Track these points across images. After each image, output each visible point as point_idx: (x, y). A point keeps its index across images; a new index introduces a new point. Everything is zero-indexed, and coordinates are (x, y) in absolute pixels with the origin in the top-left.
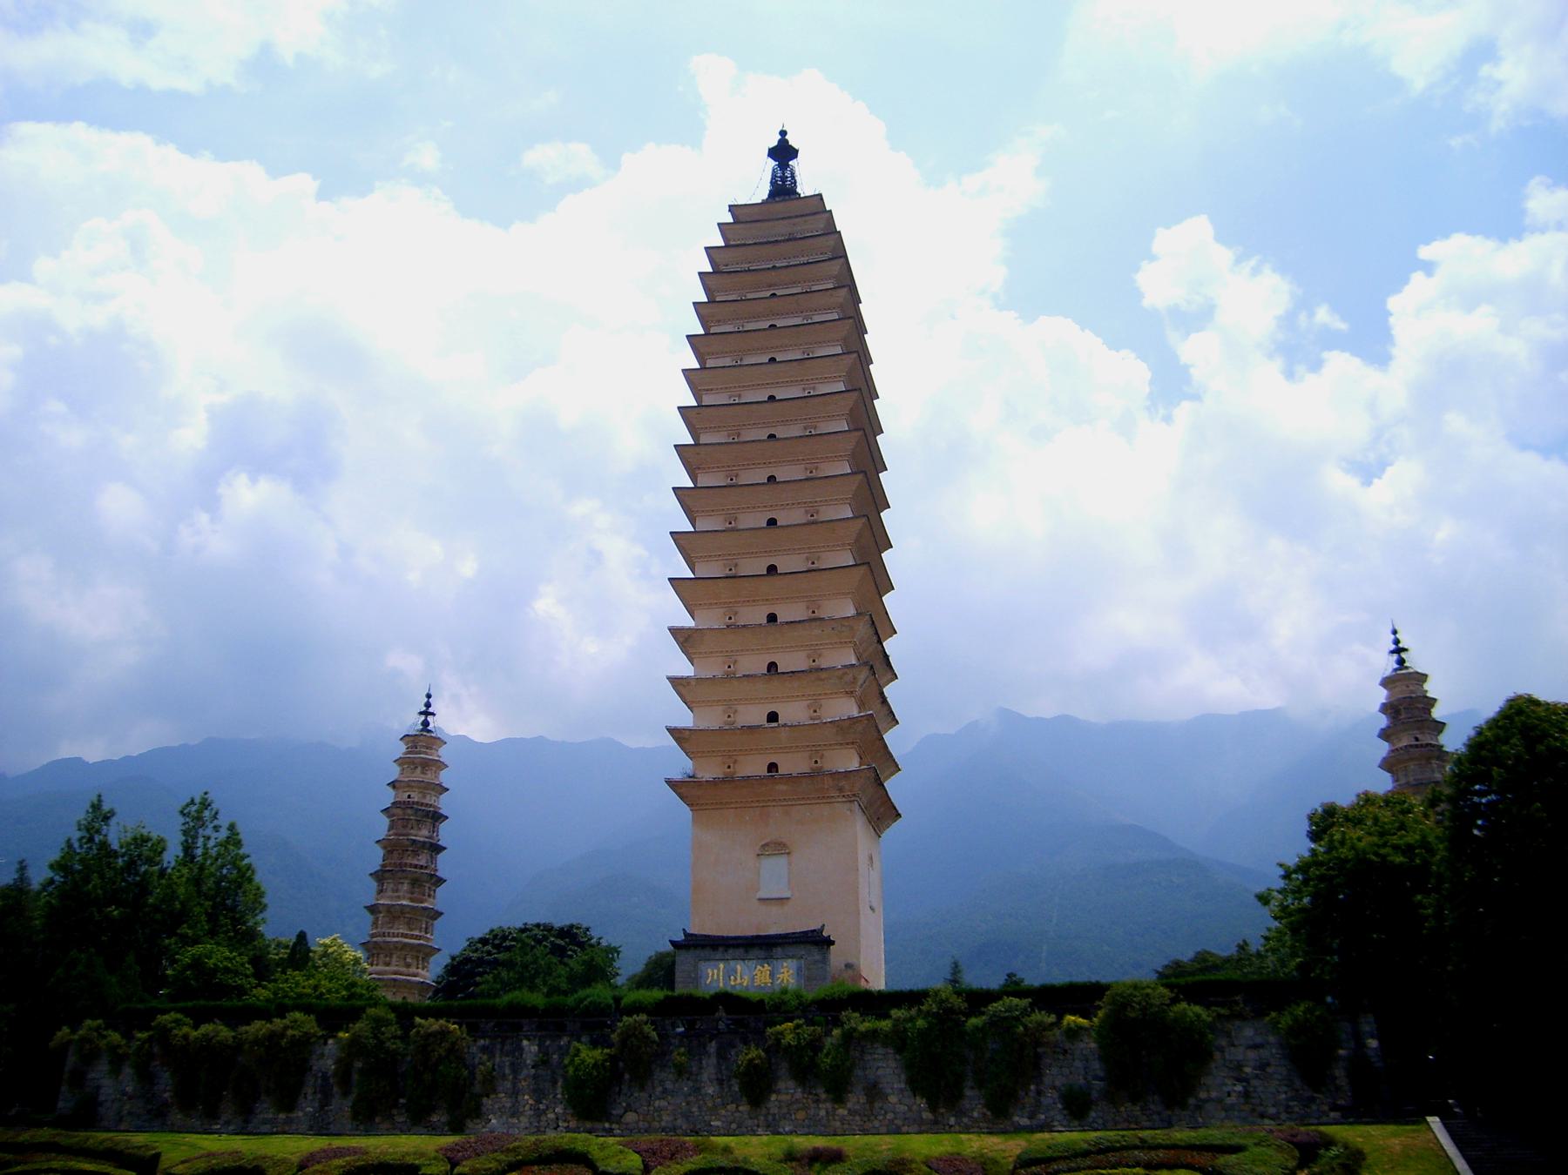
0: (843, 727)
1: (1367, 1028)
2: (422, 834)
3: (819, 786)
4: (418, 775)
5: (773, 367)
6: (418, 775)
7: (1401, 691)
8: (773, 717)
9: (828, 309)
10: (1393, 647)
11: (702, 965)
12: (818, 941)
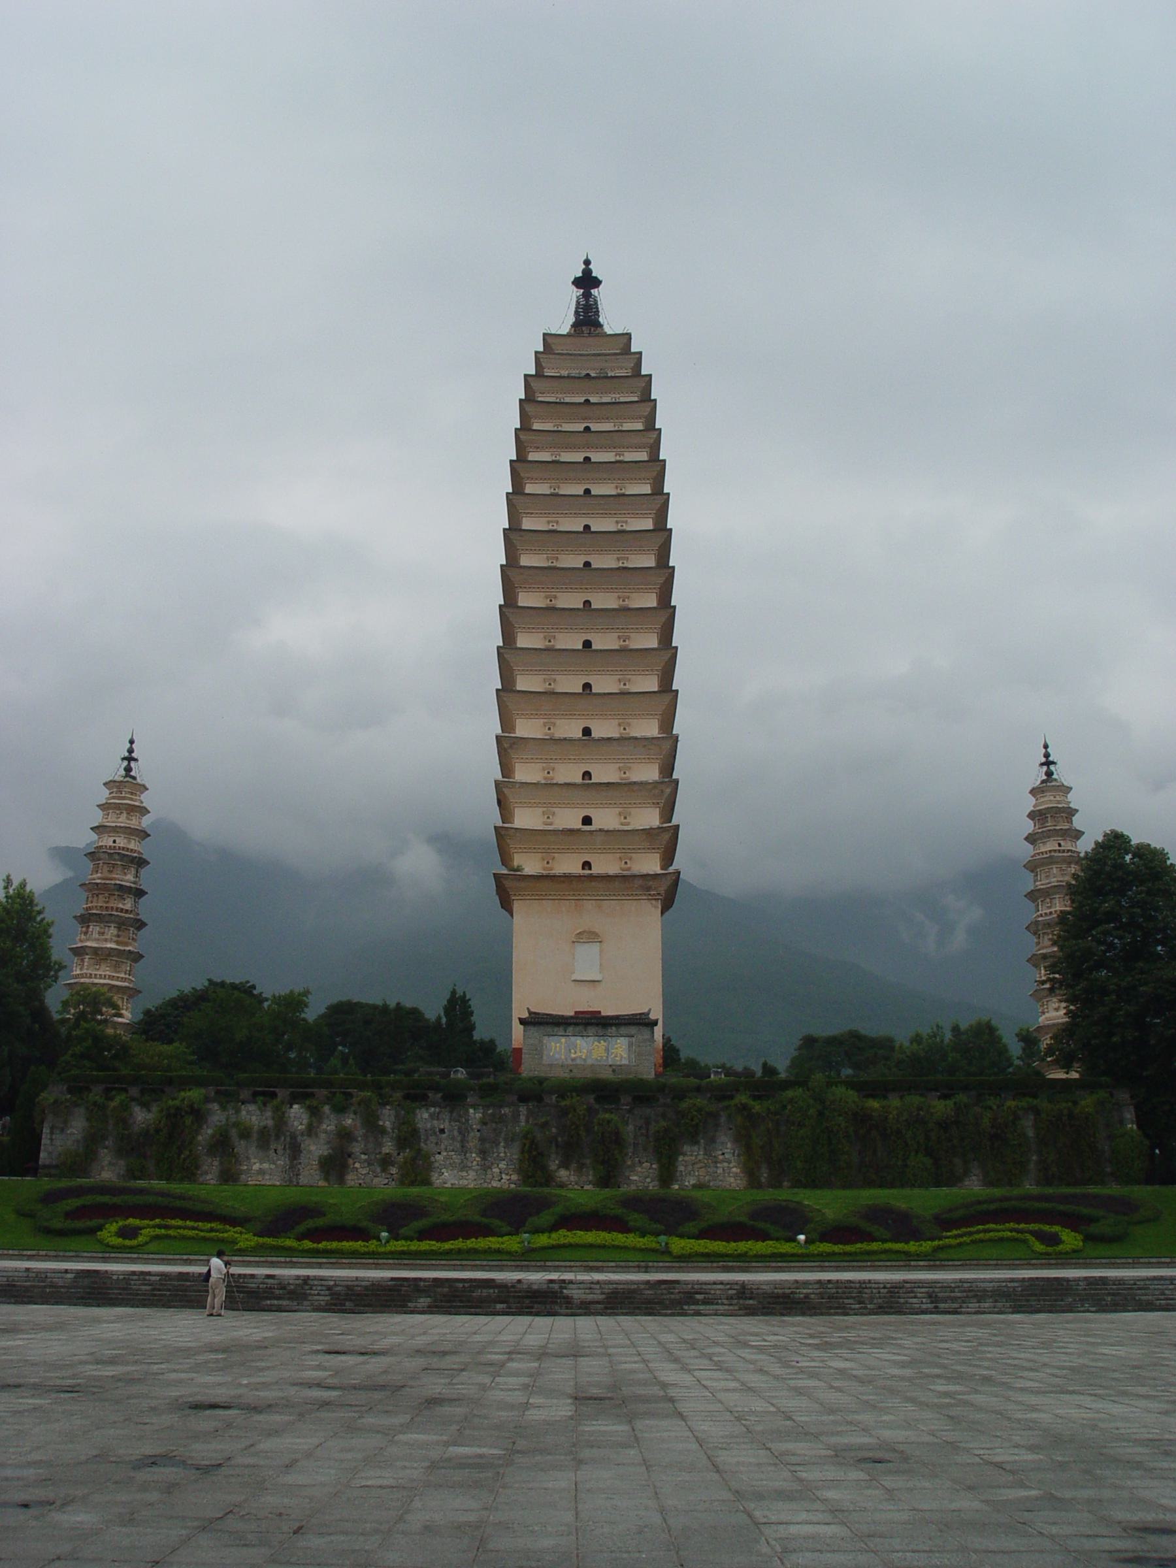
0: (649, 833)
1: (1128, 1116)
2: (128, 879)
3: (627, 884)
4: (122, 820)
5: (588, 500)
6: (122, 820)
7: (1049, 801)
8: (587, 821)
9: (638, 447)
10: (1044, 760)
11: (545, 1039)
12: (642, 1022)
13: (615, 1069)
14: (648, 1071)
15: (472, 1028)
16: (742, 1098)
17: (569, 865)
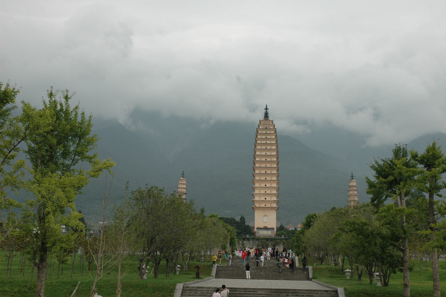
3: (271, 208)
8: (266, 199)
12: (273, 229)
13: (269, 235)
14: (273, 236)
15: (245, 223)
16: (284, 240)
17: (263, 205)
